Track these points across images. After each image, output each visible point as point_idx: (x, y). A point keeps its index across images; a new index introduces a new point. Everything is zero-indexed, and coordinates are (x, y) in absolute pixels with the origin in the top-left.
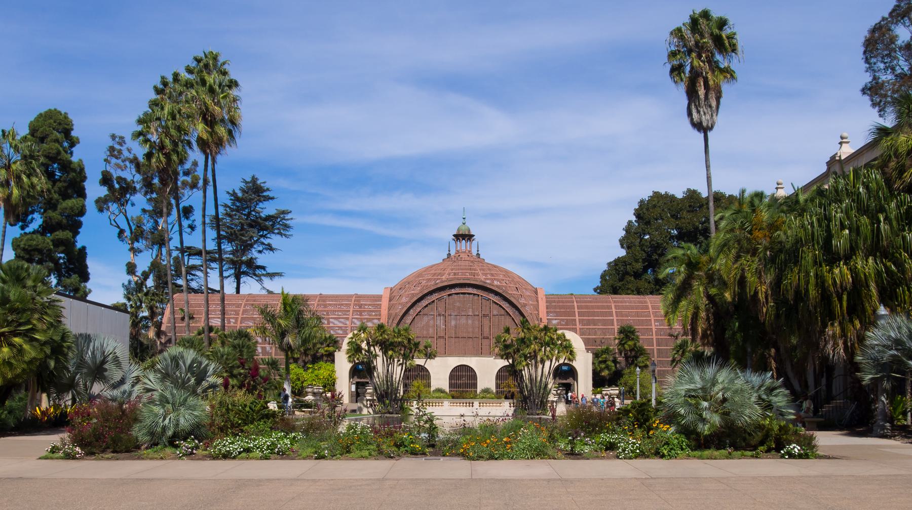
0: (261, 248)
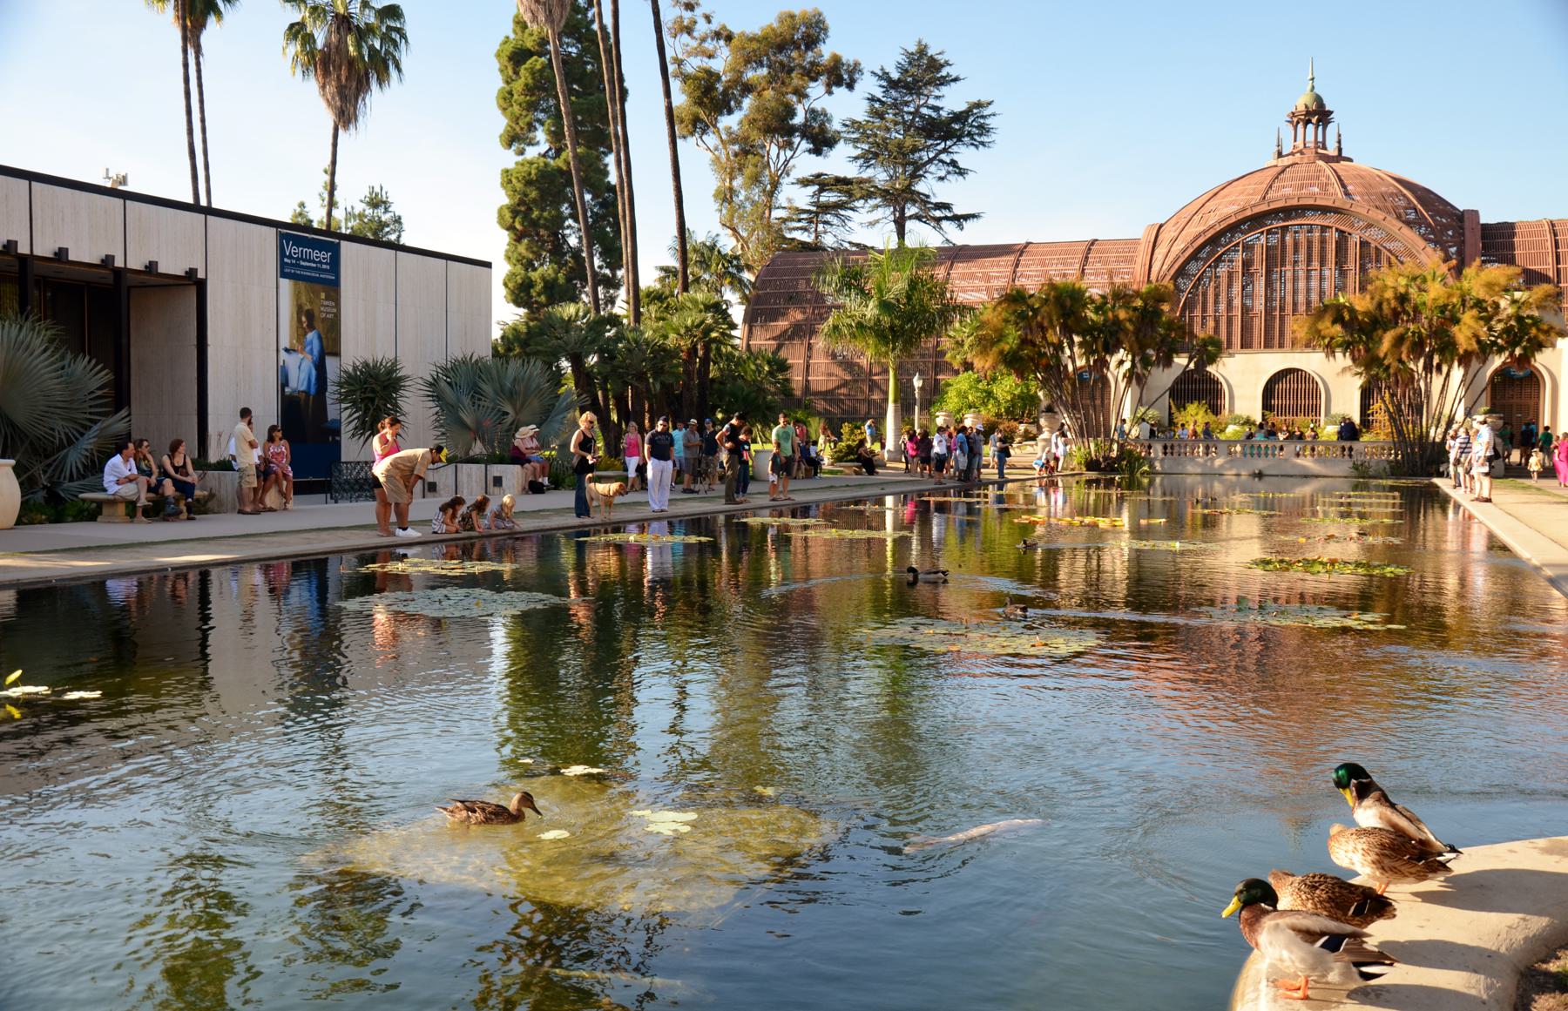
0: (942, 173)
